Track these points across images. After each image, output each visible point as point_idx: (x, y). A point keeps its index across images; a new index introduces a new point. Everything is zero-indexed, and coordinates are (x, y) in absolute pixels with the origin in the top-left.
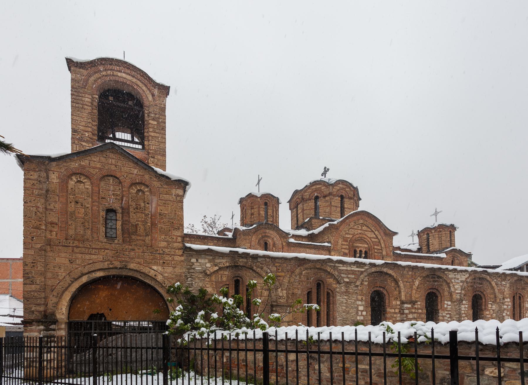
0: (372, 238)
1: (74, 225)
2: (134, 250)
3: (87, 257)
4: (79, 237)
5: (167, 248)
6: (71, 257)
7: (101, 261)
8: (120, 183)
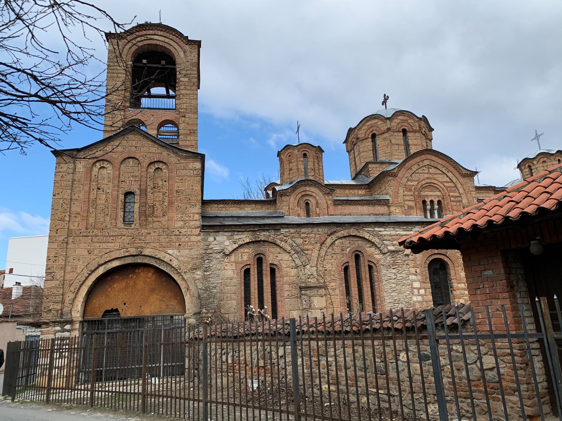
0: (444, 182)
1: (95, 213)
2: (150, 234)
3: (105, 245)
4: (99, 225)
5: (183, 228)
6: (89, 247)
7: (118, 250)
8: (139, 163)
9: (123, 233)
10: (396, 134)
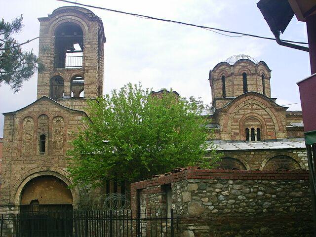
3: (30, 165)
9: (40, 159)
10: (238, 77)
